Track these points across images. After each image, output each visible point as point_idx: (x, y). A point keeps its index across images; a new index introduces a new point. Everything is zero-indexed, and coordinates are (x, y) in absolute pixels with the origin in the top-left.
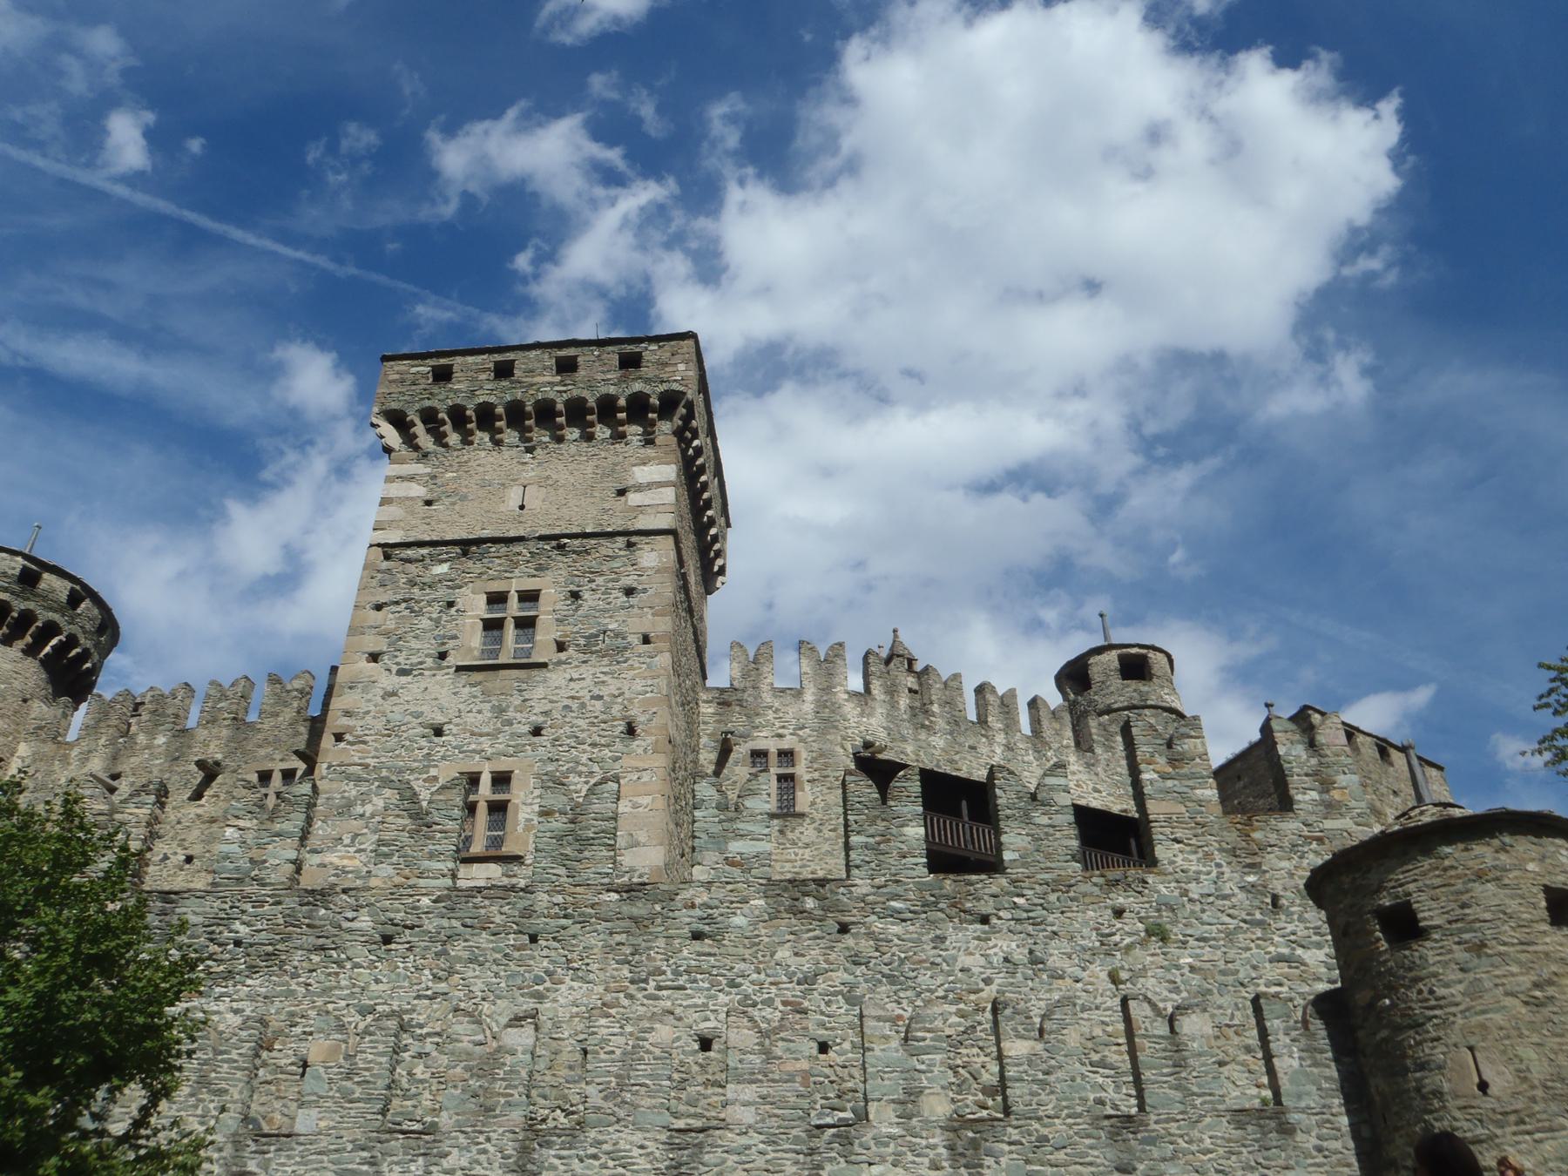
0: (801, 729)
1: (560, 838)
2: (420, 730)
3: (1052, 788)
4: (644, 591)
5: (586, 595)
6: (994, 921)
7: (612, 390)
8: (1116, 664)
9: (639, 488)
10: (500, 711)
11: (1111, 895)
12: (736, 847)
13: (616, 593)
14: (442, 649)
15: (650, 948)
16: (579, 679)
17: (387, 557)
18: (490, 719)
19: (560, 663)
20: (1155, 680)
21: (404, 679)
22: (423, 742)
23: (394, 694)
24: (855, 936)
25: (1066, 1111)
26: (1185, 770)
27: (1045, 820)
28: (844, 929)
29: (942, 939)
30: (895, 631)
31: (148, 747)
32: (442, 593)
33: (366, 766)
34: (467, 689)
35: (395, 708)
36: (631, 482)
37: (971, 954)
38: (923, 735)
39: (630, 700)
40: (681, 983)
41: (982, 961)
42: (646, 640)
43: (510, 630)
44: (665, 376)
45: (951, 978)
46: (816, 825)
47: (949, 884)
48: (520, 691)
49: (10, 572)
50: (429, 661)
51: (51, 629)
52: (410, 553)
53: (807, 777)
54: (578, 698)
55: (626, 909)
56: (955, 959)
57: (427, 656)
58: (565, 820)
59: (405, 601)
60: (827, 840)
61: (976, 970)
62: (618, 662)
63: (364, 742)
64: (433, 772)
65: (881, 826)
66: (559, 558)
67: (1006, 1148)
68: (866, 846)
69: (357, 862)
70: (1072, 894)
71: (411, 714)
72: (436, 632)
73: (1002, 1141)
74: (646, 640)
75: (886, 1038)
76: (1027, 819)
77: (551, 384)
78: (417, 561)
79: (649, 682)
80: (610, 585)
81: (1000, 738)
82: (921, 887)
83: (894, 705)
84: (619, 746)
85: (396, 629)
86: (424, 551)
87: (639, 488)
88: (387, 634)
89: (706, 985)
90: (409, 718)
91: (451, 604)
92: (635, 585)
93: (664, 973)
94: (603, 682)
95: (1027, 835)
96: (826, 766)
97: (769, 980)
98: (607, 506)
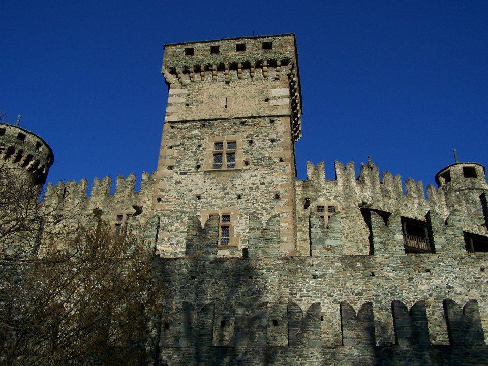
0: (337, 197)
1: (258, 239)
2: (191, 197)
3: (454, 220)
4: (279, 140)
5: (255, 142)
6: (431, 271)
7: (261, 57)
8: (462, 171)
9: (274, 98)
10: (223, 189)
11: (479, 263)
12: (328, 242)
13: (267, 141)
14: (198, 164)
15: (297, 281)
16: (255, 176)
17: (173, 127)
18: (220, 192)
19: (246, 170)
20: (478, 177)
22: (193, 201)
23: (180, 182)
24: (377, 277)
25: (476, 343)
27: (451, 232)
28: (373, 274)
29: (411, 279)
32: (196, 141)
33: (171, 211)
34: (209, 180)
35: (181, 188)
36: (270, 96)
37: (424, 284)
38: (386, 200)
39: (276, 185)
40: (310, 295)
41: (428, 288)
42: (281, 160)
43: (225, 157)
44: (282, 51)
45: (416, 294)
46: (345, 236)
47: (413, 257)
48: (231, 181)
50: (193, 169)
52: (181, 125)
54: (255, 184)
55: (286, 267)
56: (417, 286)
57: (192, 167)
58: (260, 232)
59: (182, 145)
60: (350, 241)
61: (426, 291)
62: (271, 169)
63: (170, 202)
65: (385, 234)
66: (243, 127)
67: (453, 356)
68: (380, 243)
69: (171, 249)
70: (463, 262)
71: (188, 190)
72: (195, 157)
73: (451, 354)
74: (281, 160)
75: (404, 314)
76: (444, 232)
77: (236, 56)
78: (184, 128)
79: (284, 177)
80: (265, 138)
81: (416, 201)
82: (402, 258)
83: (374, 187)
84: (273, 203)
85: (178, 156)
86: (187, 125)
87: (274, 98)
88: (175, 157)
89: (319, 296)
90: (186, 192)
91: (200, 146)
92: (275, 138)
93: (303, 291)
94: (265, 177)
95: (444, 238)
96: (348, 212)
97: (344, 294)
98: (261, 105)
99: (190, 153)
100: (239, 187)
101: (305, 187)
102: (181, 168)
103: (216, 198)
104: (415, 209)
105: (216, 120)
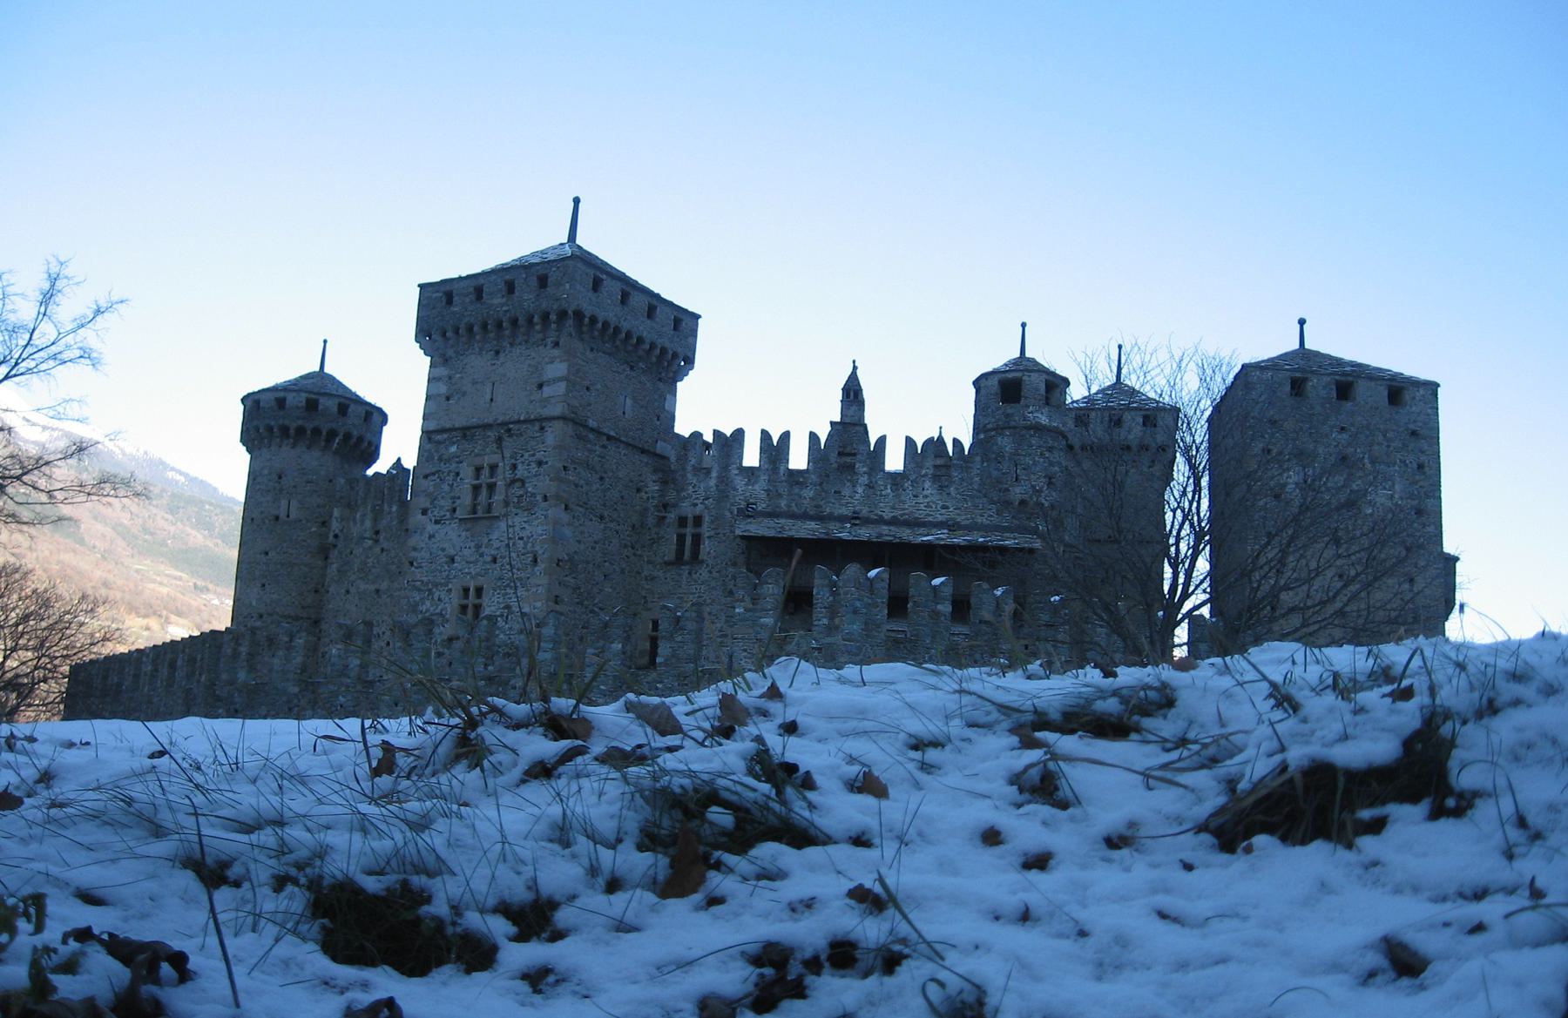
2: (444, 559)
5: (520, 467)
10: (478, 547)
21: (439, 526)
26: (759, 607)
30: (854, 362)
31: (390, 513)
33: (423, 582)
36: (545, 378)
49: (300, 405)
51: (332, 434)
52: (439, 437)
53: (707, 534)
59: (438, 472)
64: (450, 586)
65: (601, 643)
68: (594, 654)
74: (545, 498)
86: (445, 436)
90: (440, 552)
99: (446, 488)
100: (496, 544)
101: (664, 482)
102: (435, 513)
103: (471, 563)
104: (858, 496)
105: (478, 427)
